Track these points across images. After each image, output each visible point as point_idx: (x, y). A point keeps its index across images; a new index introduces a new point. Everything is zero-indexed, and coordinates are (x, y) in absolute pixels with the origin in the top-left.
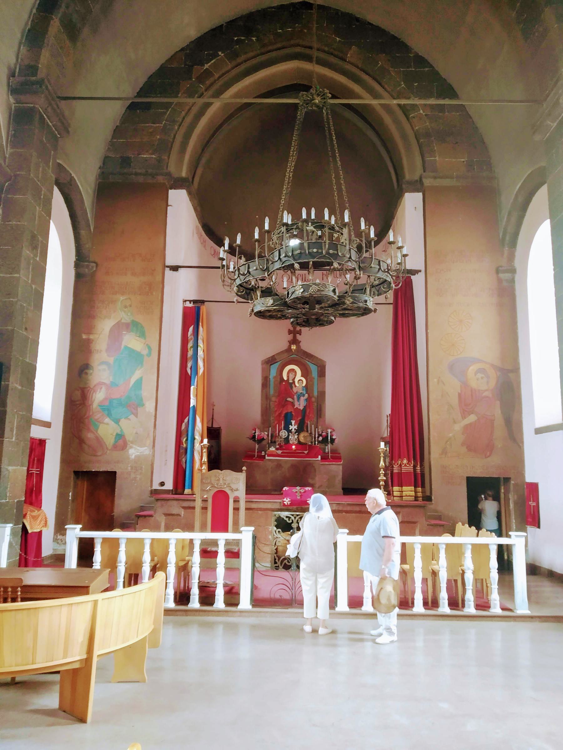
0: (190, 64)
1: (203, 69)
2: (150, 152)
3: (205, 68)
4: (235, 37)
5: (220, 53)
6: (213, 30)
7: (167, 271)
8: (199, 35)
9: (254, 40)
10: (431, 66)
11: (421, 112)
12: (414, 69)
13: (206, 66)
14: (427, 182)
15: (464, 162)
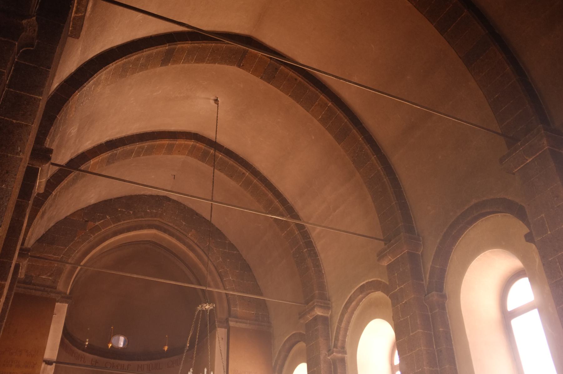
0: (86, 219)
1: (95, 224)
2: (49, 274)
3: (96, 224)
4: (119, 208)
5: (108, 217)
6: (106, 201)
7: (43, 365)
8: (96, 202)
9: (131, 213)
10: (238, 251)
11: (231, 278)
12: (228, 251)
13: (97, 223)
14: (232, 324)
15: (253, 314)
